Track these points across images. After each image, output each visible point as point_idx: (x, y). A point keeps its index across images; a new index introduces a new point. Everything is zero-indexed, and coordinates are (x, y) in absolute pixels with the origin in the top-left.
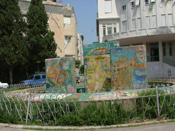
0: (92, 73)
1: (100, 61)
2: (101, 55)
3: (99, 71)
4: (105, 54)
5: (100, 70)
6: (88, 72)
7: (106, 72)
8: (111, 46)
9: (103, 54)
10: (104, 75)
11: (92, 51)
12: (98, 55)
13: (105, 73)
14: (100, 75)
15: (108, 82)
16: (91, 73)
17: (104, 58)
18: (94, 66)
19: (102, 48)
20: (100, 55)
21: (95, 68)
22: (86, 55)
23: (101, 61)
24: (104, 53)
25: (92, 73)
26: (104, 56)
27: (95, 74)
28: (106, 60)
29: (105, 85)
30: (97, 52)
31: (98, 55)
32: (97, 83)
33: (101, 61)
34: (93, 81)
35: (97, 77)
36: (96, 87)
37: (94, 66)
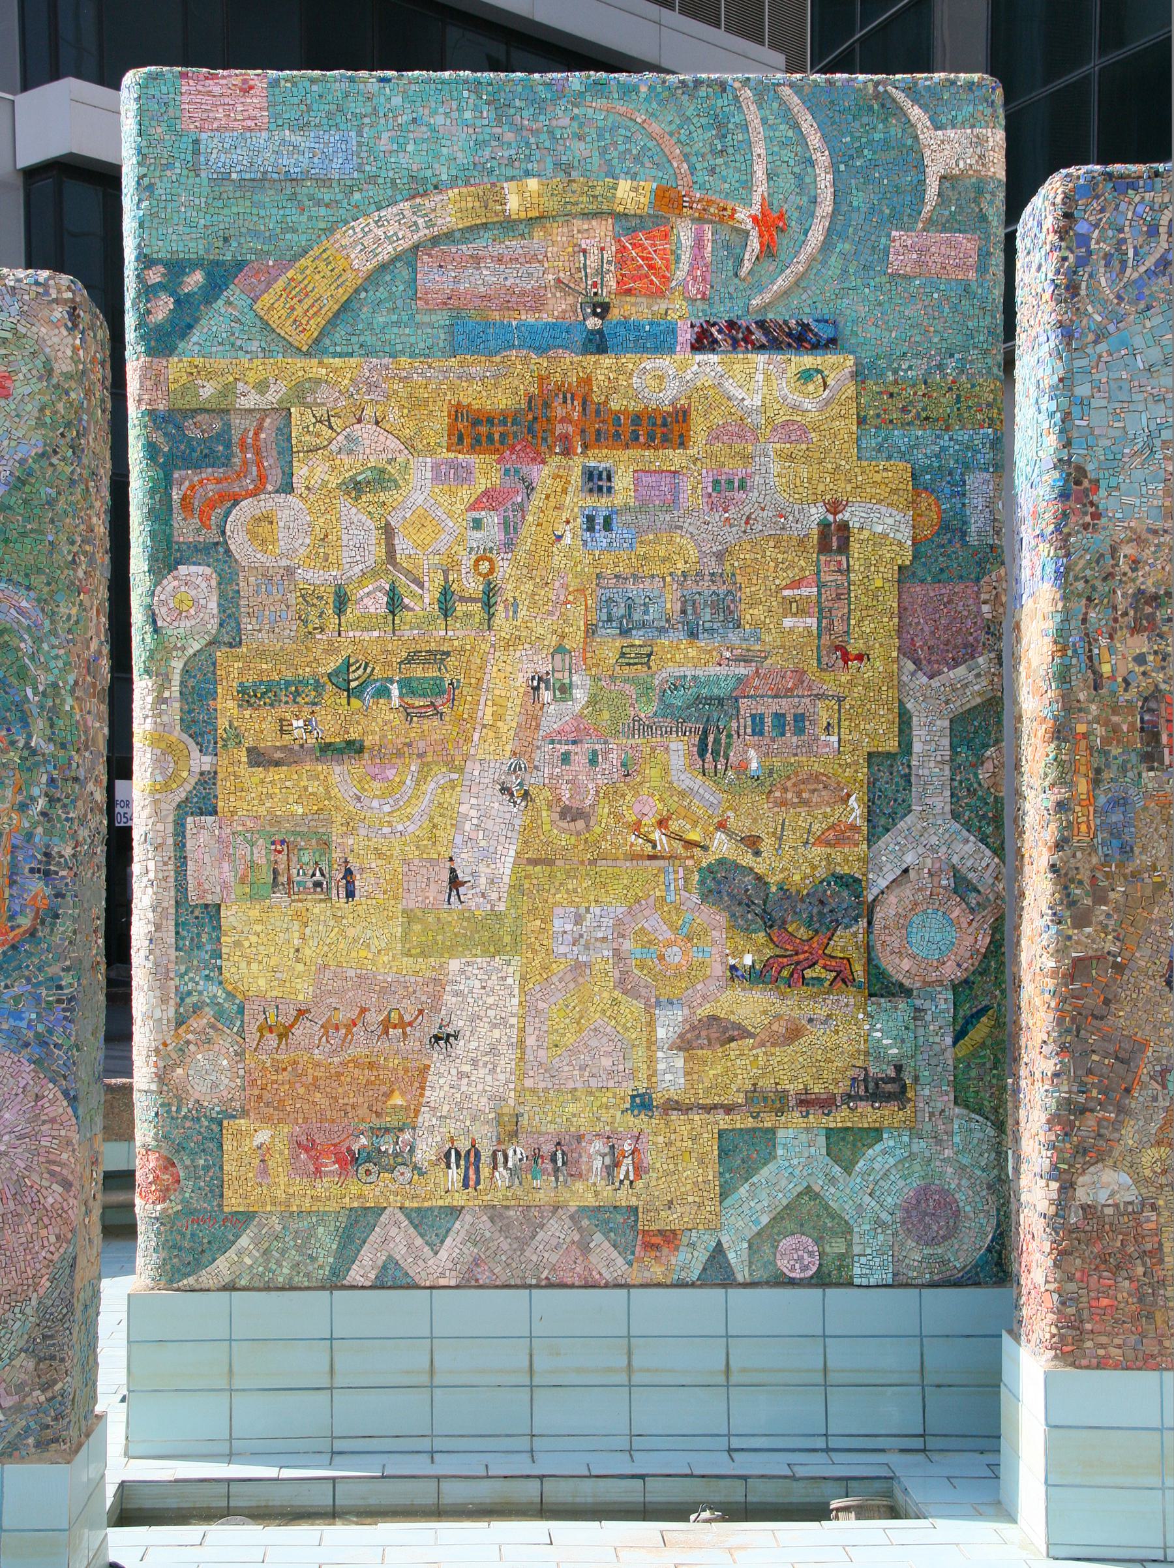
0: (354, 748)
1: (578, 502)
2: (598, 343)
3: (532, 721)
4: (703, 342)
5: (565, 690)
6: (260, 728)
7: (709, 748)
8: (841, 159)
9: (657, 340)
10: (652, 808)
11: (372, 238)
12: (542, 341)
13: (678, 750)
14: (570, 814)
15: (757, 976)
16: (327, 751)
17: (666, 428)
18: (422, 601)
19: (629, 194)
20: (569, 365)
21: (439, 657)
22: (216, 320)
23: (597, 482)
24: (680, 313)
25: (354, 748)
26: (664, 397)
27: (441, 775)
28: (725, 488)
29: (684, 1044)
30: (514, 278)
31: (542, 341)
32: (483, 994)
33: (597, 482)
34: (365, 941)
35: (493, 868)
36: (440, 1088)
37: (422, 601)
